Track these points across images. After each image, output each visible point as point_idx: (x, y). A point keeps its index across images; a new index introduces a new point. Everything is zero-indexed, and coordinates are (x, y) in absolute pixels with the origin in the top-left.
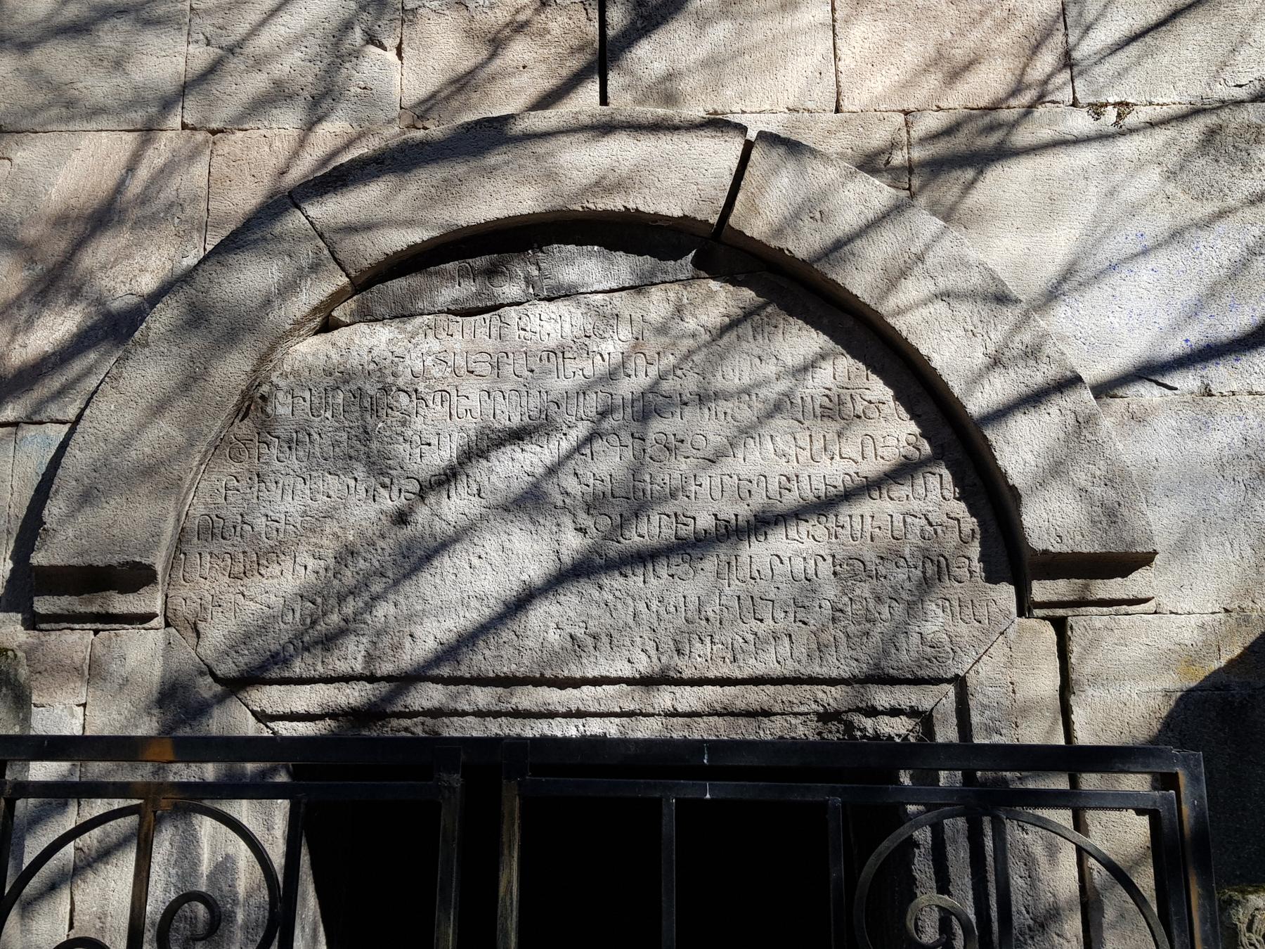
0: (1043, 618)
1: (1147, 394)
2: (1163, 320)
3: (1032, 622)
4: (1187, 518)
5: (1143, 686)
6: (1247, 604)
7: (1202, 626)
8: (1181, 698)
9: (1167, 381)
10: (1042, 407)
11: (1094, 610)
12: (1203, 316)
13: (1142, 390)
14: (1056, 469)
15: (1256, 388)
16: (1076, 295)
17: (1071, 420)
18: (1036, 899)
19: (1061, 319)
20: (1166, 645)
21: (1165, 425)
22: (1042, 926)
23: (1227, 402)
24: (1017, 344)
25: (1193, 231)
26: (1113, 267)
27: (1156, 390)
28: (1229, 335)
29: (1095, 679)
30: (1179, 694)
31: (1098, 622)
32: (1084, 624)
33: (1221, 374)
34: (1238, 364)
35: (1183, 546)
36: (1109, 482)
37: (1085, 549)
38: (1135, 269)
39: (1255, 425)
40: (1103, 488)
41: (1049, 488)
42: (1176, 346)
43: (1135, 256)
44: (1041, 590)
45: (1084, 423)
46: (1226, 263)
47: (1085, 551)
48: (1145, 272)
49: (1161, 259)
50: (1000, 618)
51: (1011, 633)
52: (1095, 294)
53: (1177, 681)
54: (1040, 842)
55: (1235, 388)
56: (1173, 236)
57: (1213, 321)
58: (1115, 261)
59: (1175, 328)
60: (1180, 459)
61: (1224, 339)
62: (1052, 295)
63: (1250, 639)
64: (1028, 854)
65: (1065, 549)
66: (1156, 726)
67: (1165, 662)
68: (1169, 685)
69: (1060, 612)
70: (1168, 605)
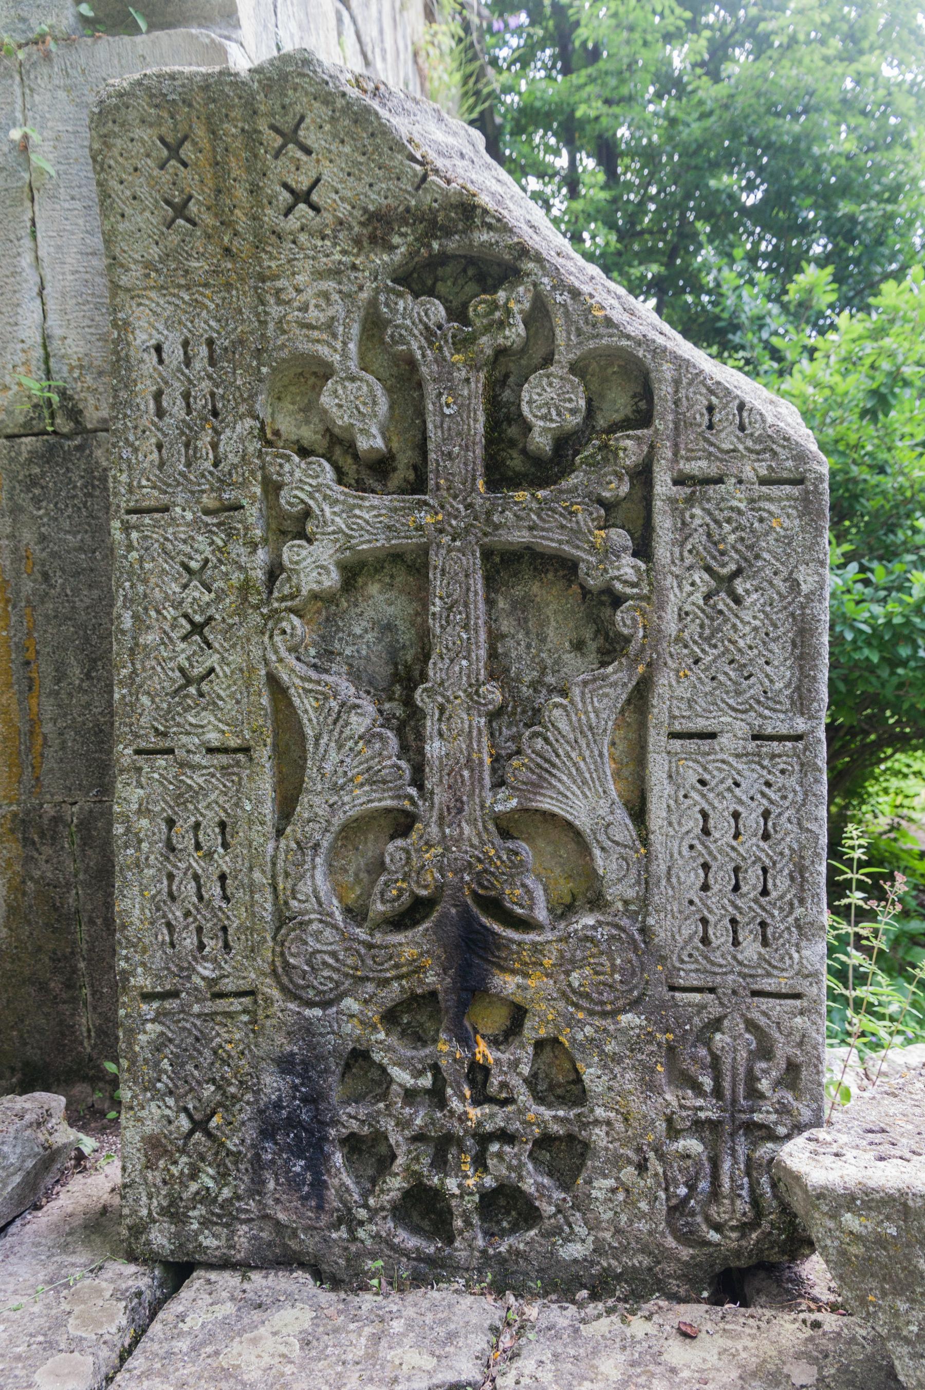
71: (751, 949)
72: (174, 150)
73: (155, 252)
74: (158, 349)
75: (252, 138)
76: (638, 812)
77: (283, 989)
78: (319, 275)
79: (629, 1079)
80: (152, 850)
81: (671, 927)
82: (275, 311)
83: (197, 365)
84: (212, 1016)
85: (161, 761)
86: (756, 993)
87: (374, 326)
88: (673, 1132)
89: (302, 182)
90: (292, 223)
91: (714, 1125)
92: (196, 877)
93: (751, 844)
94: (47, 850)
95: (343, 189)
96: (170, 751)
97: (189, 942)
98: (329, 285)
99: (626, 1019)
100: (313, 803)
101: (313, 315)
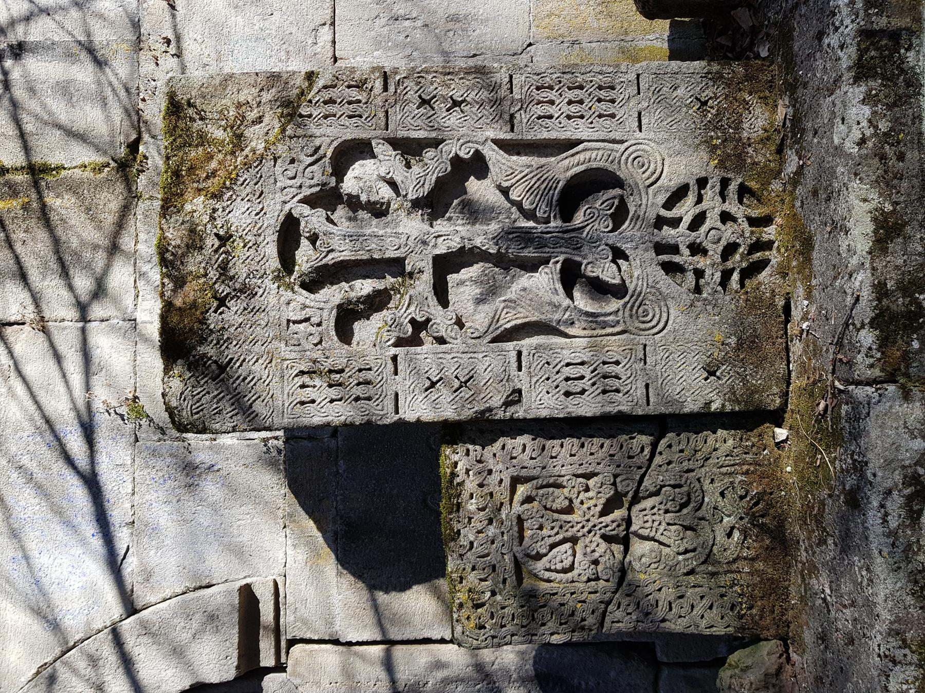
0: (287, 653)
1: (131, 567)
2: (78, 551)
3: (290, 663)
4: (221, 548)
5: (334, 591)
6: (280, 513)
7: (295, 546)
8: (342, 566)
9: (123, 552)
10: (134, 659)
11: (282, 621)
12: (76, 522)
13: (129, 570)
14: (178, 653)
15: (130, 491)
16: (57, 610)
17: (145, 639)
18: (470, 679)
19: (74, 623)
20: (307, 572)
21: (153, 557)
22: (487, 675)
23: (139, 513)
24: (88, 672)
25: (12, 521)
26: (37, 583)
27: (129, 559)
28: (90, 505)
29: (330, 623)
30: (340, 567)
31: (290, 618)
32: (291, 629)
33: (118, 514)
34: (112, 501)
35: (239, 552)
36: (189, 617)
37: (236, 640)
38: (39, 566)
39: (156, 495)
40: (193, 621)
41: (192, 660)
42: (97, 543)
43: (28, 564)
44: (267, 659)
45: (146, 629)
46: (37, 500)
47: (237, 640)
48: (42, 560)
49: (33, 546)
50: (286, 688)
51: (297, 681)
52: (57, 596)
53: (330, 564)
54: (434, 673)
55: (129, 505)
56: (15, 536)
57: (79, 516)
58: (33, 581)
59: (83, 542)
60: (178, 550)
61: (93, 509)
62: (55, 626)
63: (303, 513)
64: (442, 682)
65: (235, 654)
66: (360, 584)
67: (317, 574)
68: (334, 572)
69: (283, 644)
70: (280, 569)
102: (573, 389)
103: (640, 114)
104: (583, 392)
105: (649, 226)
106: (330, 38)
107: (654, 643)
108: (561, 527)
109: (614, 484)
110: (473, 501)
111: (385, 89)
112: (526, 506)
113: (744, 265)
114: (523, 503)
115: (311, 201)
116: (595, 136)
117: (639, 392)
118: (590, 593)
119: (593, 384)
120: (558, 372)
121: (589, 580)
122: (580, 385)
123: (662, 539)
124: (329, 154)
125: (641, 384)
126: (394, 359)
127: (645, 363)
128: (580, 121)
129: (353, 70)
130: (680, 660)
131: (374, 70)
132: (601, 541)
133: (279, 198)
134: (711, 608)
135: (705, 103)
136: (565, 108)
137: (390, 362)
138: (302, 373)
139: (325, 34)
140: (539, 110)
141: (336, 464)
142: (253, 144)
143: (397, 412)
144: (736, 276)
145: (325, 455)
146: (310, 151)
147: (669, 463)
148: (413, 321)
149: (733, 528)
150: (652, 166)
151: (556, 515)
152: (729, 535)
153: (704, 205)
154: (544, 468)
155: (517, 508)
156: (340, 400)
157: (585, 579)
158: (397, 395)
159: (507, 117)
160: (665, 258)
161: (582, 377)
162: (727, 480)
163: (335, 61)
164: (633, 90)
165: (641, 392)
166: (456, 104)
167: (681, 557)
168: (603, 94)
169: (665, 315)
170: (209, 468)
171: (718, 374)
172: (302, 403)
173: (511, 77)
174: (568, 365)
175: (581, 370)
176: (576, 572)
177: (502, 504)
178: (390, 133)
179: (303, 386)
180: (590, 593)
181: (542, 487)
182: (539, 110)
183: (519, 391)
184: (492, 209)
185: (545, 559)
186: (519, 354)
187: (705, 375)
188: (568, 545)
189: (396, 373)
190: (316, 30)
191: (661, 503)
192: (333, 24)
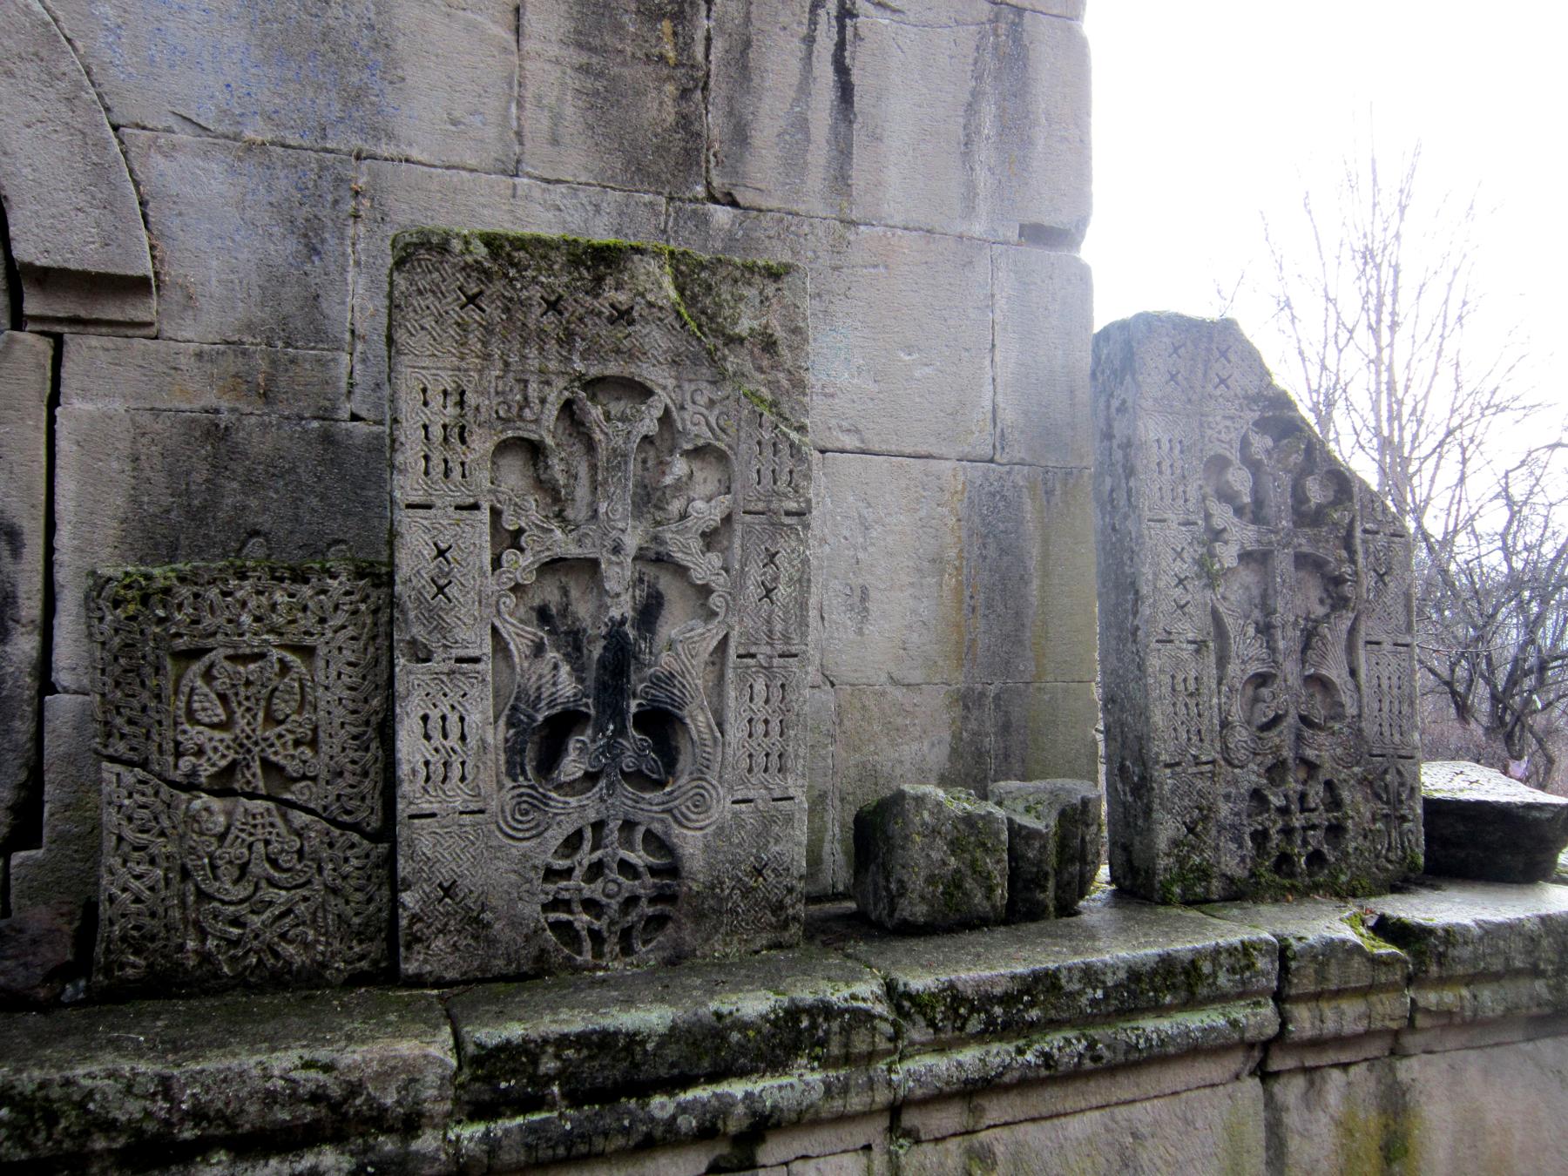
0: (42, 333)
69: (57, 329)
71: (1397, 737)
72: (1176, 350)
73: (1160, 394)
74: (1158, 441)
75: (1209, 350)
76: (1353, 673)
77: (1225, 759)
78: (1225, 417)
79: (1359, 797)
80: (1166, 690)
81: (1369, 729)
82: (1209, 432)
83: (1177, 451)
84: (1194, 775)
85: (1169, 646)
86: (1401, 757)
87: (1245, 443)
88: (1374, 820)
89: (1224, 374)
90: (1218, 392)
91: (1386, 816)
92: (1186, 705)
93: (1395, 691)
94: (976, 713)
95: (1243, 382)
96: (1171, 641)
97: (1185, 736)
98: (1228, 423)
99: (1356, 769)
100: (1233, 668)
101: (1223, 436)
102: (431, 724)
103: (750, 801)
104: (427, 737)
105: (626, 813)
106: (848, 448)
107: (39, 847)
108: (248, 709)
109: (304, 777)
110: (286, 599)
111: (788, 513)
112: (277, 667)
113: (577, 925)
114: (281, 660)
115: (666, 419)
116: (730, 751)
117: (425, 806)
118: (160, 745)
119: (437, 750)
120: (453, 707)
121: (177, 744)
122: (436, 735)
123: (231, 837)
124: (717, 444)
125: (435, 807)
126: (475, 507)
127: (461, 813)
128: (746, 734)
129: (807, 477)
130: (13, 883)
131: (808, 501)
132: (229, 759)
133: (671, 383)
134: (137, 900)
135: (760, 873)
136: (761, 716)
137: (472, 500)
138: (463, 393)
139: (850, 441)
140: (760, 686)
141: (315, 418)
142: (731, 358)
143: (409, 506)
144: (564, 916)
145: (327, 403)
146: (722, 422)
147: (331, 845)
148: (520, 532)
149: (243, 925)
150: (693, 817)
151: (263, 703)
152: (236, 922)
153: (649, 880)
154: (327, 688)
155: (275, 654)
156: (427, 437)
157: (180, 738)
158: (428, 507)
159: (753, 650)
160: (588, 834)
161: (445, 736)
162: (308, 918)
163: (823, 452)
164: (777, 794)
165: (426, 807)
166: (769, 591)
167: (206, 860)
168: (774, 758)
169: (520, 835)
170: (315, 249)
171: (447, 900)
172: (424, 390)
173: (795, 656)
174: (462, 719)
175: (454, 732)
176: (187, 727)
177: (281, 634)
178: (739, 517)
179: (445, 393)
180: (160, 745)
181: (302, 687)
182: (760, 686)
183: (427, 660)
184: (653, 632)
185: (206, 689)
186: (476, 660)
187: (446, 884)
188: (224, 717)
189: (458, 508)
190: (857, 431)
191: (278, 835)
192: (863, 452)
